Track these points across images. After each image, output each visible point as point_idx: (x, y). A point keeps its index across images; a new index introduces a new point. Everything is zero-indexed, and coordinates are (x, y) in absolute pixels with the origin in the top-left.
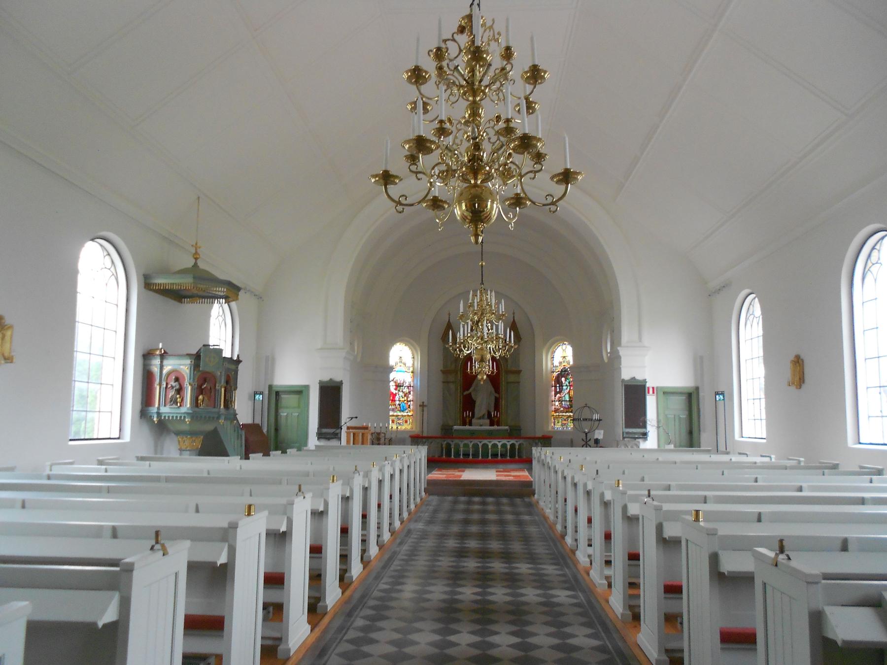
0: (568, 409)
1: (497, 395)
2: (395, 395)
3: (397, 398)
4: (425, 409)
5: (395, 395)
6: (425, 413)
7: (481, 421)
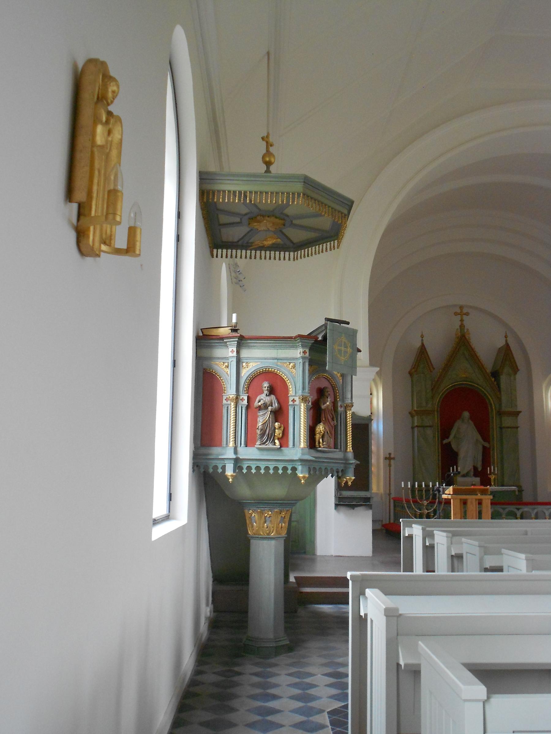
1: (486, 445)
6: (392, 468)
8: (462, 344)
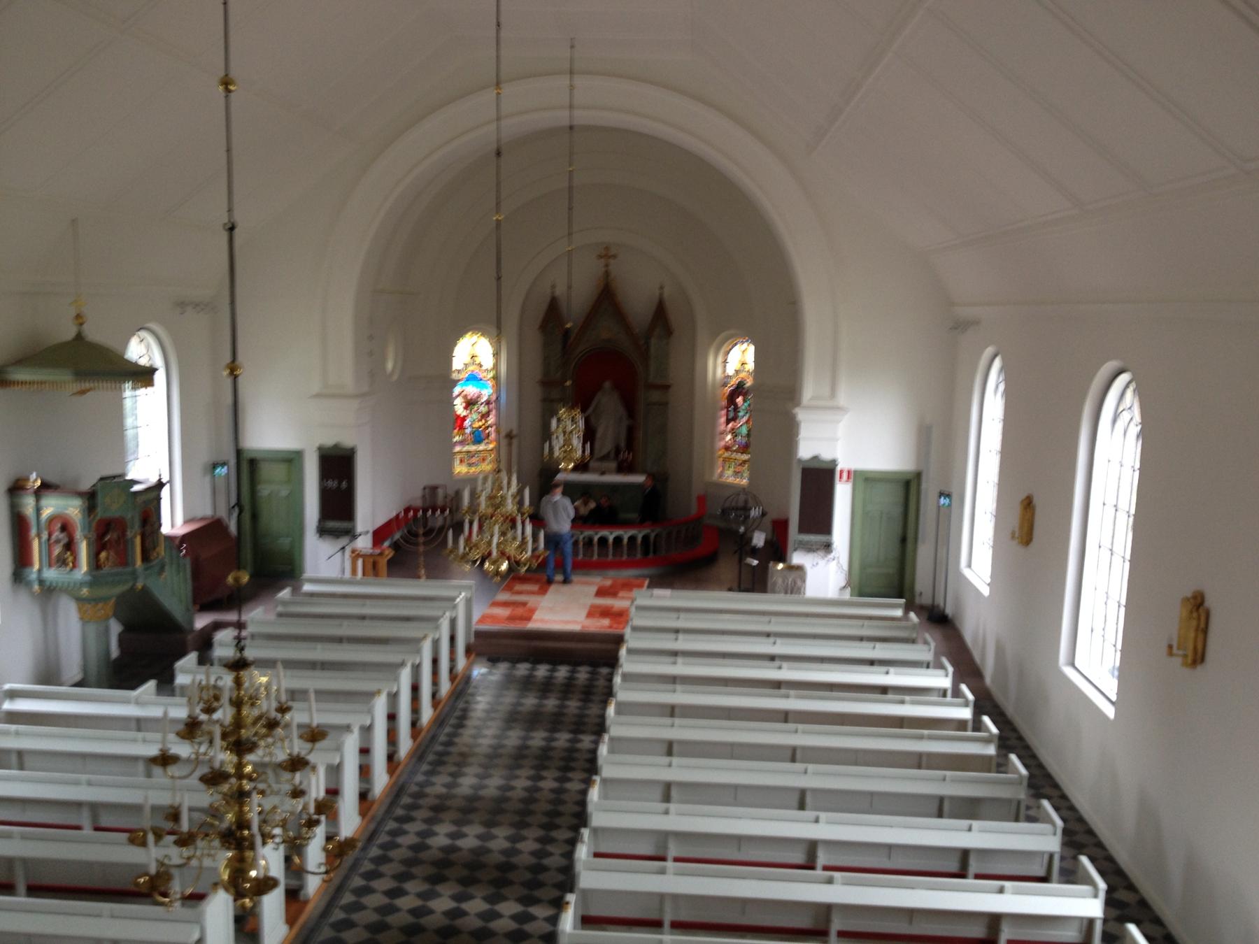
0: (744, 449)
2: (464, 419)
3: (467, 423)
4: (515, 442)
5: (464, 419)
7: (606, 465)
8: (607, 298)
